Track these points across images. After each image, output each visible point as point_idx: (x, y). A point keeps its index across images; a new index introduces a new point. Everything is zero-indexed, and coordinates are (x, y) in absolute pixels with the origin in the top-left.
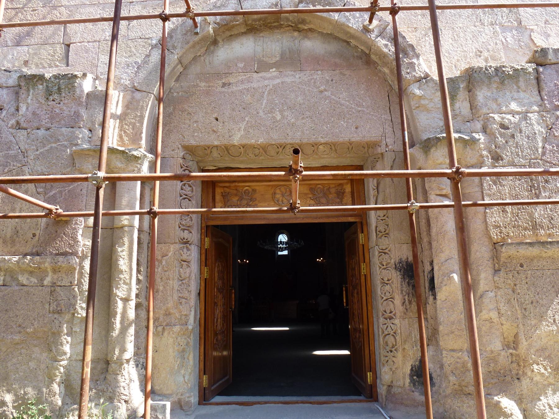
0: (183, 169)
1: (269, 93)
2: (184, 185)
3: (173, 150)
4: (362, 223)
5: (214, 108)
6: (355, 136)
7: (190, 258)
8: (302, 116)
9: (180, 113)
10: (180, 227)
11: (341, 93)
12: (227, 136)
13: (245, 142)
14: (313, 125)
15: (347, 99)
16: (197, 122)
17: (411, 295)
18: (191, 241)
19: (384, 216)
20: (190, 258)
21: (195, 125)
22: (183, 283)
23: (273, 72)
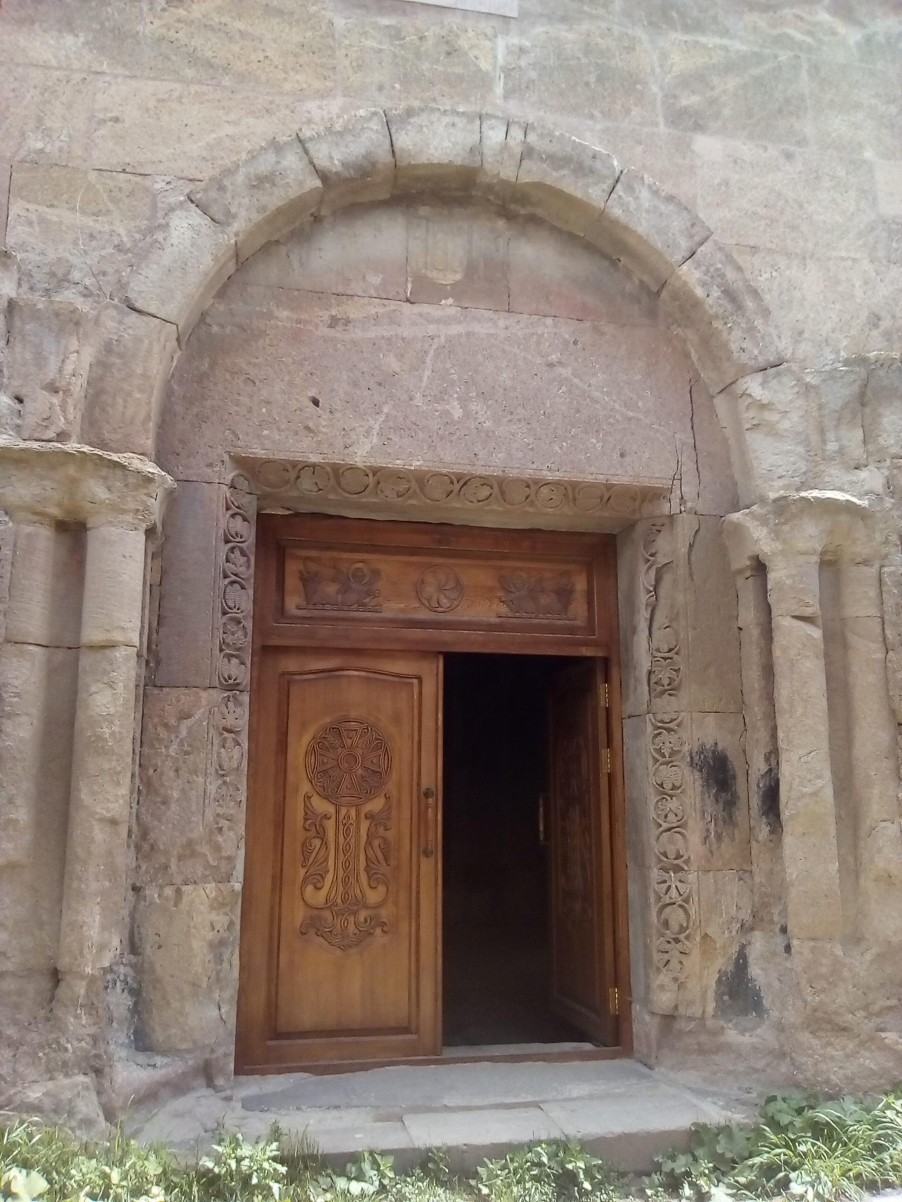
0: (230, 512)
1: (437, 355)
2: (232, 550)
3: (210, 465)
4: (606, 661)
5: (309, 375)
6: (618, 472)
7: (240, 722)
8: (509, 418)
9: (228, 376)
10: (221, 650)
11: (594, 375)
12: (339, 444)
13: (380, 461)
14: (532, 440)
15: (605, 389)
16: (269, 403)
17: (721, 823)
18: (244, 684)
19: (670, 650)
20: (240, 722)
21: (264, 410)
22: (225, 782)
23: (448, 307)
